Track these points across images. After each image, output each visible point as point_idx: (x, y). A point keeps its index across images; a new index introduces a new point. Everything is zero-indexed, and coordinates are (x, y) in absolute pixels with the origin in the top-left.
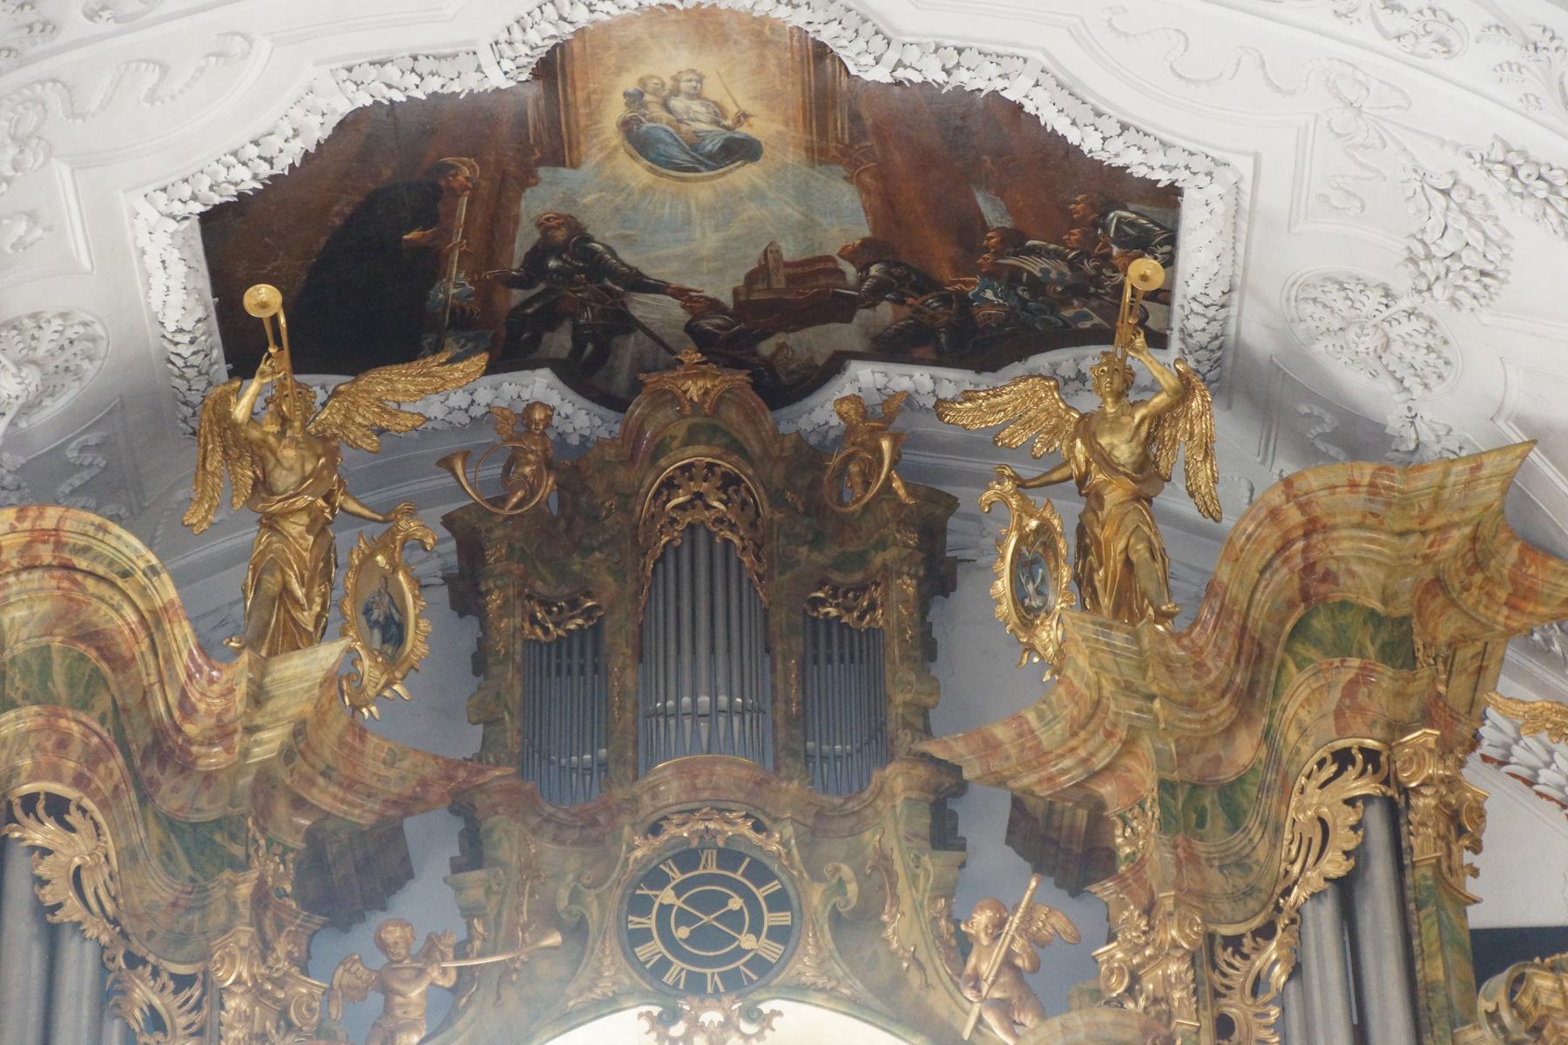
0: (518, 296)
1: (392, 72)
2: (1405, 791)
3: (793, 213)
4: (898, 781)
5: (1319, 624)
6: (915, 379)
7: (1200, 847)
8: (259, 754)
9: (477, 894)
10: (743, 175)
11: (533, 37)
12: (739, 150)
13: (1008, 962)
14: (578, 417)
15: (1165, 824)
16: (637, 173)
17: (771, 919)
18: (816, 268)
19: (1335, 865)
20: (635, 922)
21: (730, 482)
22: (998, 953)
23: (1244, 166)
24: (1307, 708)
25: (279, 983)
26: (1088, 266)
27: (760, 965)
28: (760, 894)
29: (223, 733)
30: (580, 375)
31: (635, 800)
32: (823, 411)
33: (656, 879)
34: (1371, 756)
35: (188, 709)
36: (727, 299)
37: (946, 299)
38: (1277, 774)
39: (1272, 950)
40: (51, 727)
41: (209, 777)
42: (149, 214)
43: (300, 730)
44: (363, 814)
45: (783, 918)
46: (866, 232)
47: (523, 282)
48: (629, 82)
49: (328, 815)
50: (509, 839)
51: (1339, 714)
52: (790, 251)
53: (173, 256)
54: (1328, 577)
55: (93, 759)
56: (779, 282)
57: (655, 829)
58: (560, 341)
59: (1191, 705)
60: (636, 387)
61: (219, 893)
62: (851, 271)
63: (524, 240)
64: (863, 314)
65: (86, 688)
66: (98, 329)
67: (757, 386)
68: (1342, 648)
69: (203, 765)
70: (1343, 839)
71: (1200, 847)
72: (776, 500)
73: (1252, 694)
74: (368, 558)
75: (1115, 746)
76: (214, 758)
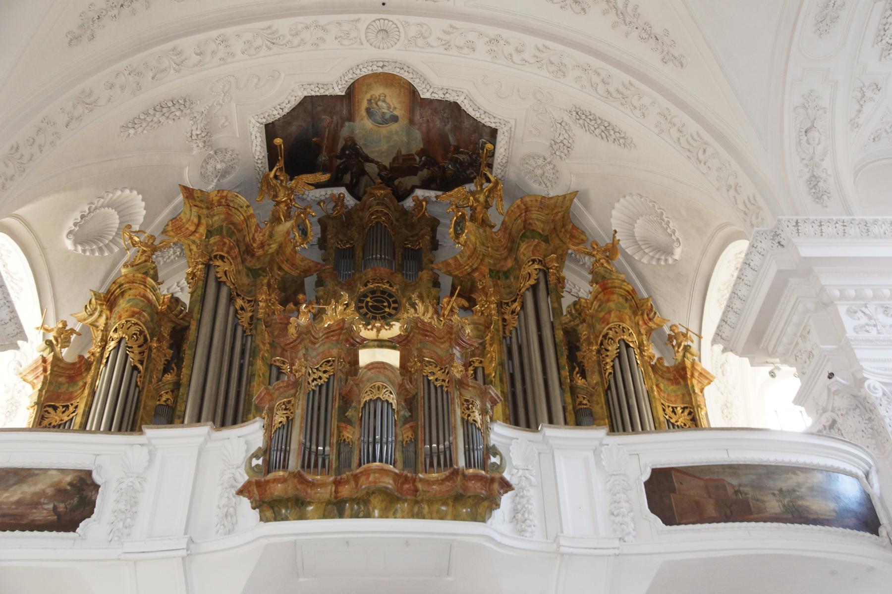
0: (339, 161)
1: (313, 87)
2: (548, 269)
3: (405, 139)
4: (425, 275)
5: (527, 234)
6: (432, 194)
7: (499, 282)
8: (271, 251)
9: (321, 293)
10: (394, 127)
11: (346, 78)
12: (395, 119)
14: (350, 201)
15: (491, 277)
16: (368, 124)
17: (393, 305)
18: (409, 157)
19: (532, 282)
20: (360, 305)
21: (386, 214)
22: (449, 307)
23: (513, 123)
24: (525, 250)
25: (273, 304)
26: (474, 156)
27: (390, 315)
28: (391, 300)
29: (262, 245)
30: (352, 190)
31: (361, 277)
32: (409, 203)
33: (366, 296)
34: (540, 261)
35: (254, 239)
36: (388, 165)
37: (439, 168)
38: (518, 264)
39: (516, 304)
40: (222, 241)
41: (258, 258)
42: (253, 121)
43: (280, 247)
44: (295, 273)
45: (396, 305)
46: (422, 146)
47: (340, 158)
48: (368, 96)
49: (286, 273)
50: (330, 284)
51: (533, 251)
52: (404, 152)
53: (258, 135)
54: (530, 224)
55: (231, 248)
56: (401, 161)
57: (366, 285)
58: (347, 178)
59: (497, 251)
60: (365, 192)
61: (259, 282)
62: (417, 158)
63: (341, 144)
64: (420, 173)
65: (231, 234)
66: (240, 157)
67: (393, 194)
68: (534, 237)
69: (257, 254)
70: (534, 276)
71: (499, 282)
72: (397, 220)
73: (512, 249)
74: (299, 215)
75: (479, 260)
76: (260, 252)
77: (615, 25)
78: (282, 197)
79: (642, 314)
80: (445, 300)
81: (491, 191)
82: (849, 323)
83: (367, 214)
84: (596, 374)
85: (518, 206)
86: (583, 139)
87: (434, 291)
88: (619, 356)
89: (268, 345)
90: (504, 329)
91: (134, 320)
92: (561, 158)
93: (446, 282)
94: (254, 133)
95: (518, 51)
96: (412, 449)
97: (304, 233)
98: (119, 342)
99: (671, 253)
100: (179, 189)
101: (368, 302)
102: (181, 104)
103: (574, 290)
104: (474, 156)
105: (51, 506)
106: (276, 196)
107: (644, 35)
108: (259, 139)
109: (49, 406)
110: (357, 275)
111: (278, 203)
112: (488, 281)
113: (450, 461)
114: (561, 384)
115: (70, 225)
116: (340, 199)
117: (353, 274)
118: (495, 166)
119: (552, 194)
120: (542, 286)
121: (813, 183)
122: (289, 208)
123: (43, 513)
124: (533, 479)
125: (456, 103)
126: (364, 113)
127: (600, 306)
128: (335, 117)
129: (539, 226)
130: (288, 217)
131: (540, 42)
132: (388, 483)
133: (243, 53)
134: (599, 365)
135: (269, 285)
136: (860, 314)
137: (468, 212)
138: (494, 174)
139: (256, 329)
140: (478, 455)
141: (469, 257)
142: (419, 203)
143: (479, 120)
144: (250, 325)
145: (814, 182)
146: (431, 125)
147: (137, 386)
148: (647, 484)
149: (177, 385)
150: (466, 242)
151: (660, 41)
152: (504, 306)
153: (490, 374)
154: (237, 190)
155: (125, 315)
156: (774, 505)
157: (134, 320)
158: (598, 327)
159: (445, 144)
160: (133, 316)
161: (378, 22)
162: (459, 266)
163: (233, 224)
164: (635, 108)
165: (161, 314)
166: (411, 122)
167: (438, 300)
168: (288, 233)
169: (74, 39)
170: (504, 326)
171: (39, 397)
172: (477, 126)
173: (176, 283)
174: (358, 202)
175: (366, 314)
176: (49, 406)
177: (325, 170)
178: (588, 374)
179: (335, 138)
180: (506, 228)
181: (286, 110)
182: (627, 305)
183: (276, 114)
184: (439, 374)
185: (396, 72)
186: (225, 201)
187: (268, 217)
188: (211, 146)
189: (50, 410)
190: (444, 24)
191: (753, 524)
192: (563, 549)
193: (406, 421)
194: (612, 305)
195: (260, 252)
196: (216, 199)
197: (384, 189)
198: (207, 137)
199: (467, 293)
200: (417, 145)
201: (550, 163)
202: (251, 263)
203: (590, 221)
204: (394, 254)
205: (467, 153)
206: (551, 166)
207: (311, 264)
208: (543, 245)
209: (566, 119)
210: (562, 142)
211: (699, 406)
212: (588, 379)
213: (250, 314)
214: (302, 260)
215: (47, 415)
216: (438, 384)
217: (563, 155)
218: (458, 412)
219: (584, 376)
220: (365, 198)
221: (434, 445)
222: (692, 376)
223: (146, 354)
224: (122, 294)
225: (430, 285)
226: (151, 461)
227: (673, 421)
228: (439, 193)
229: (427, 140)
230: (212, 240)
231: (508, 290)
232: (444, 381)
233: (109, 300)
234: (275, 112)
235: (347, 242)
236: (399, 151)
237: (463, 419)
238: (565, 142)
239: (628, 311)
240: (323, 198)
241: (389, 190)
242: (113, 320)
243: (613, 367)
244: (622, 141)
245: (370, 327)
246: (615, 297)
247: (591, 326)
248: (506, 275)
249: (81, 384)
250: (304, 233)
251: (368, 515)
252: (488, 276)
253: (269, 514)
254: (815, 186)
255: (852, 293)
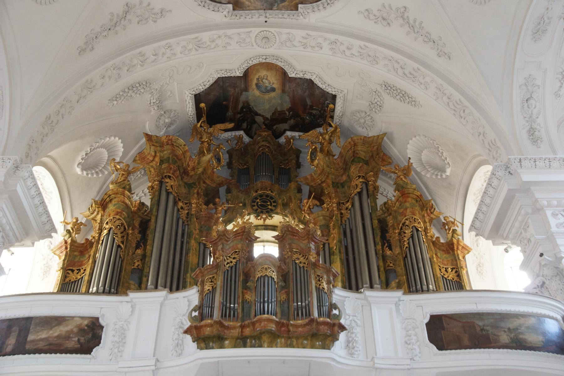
0: (239, 116)
1: (223, 72)
2: (368, 181)
3: (280, 102)
4: (293, 185)
5: (356, 160)
6: (296, 134)
7: (338, 190)
8: (199, 172)
9: (229, 197)
10: (273, 94)
11: (244, 66)
13: (309, 207)
14: (246, 139)
15: (333, 187)
16: (257, 93)
17: (273, 204)
18: (282, 112)
20: (253, 204)
21: (268, 147)
22: (308, 206)
23: (346, 91)
24: (354, 170)
25: (200, 205)
26: (322, 111)
27: (271, 210)
28: (272, 201)
29: (193, 169)
30: (247, 132)
31: (253, 187)
32: (282, 140)
33: (257, 198)
34: (363, 176)
35: (188, 165)
36: (269, 118)
38: (350, 178)
39: (349, 203)
40: (169, 166)
41: (191, 176)
42: (187, 93)
43: (204, 170)
44: (214, 185)
45: (275, 204)
46: (290, 106)
47: (240, 113)
48: (257, 77)
49: (208, 185)
50: (235, 192)
51: (359, 171)
53: (190, 101)
54: (357, 154)
55: (175, 171)
56: (277, 115)
57: (257, 192)
58: (245, 125)
59: (337, 170)
60: (255, 134)
61: (192, 191)
62: (287, 113)
63: (241, 105)
64: (289, 121)
65: (175, 162)
66: (179, 114)
67: (273, 134)
68: (359, 162)
69: (190, 174)
70: (360, 186)
71: (338, 190)
72: (275, 151)
73: (346, 169)
74: (216, 149)
75: (326, 177)
76: (192, 173)
77: (408, 33)
78: (205, 139)
79: (427, 210)
80: (305, 201)
81: (333, 133)
82: (553, 222)
83: (257, 147)
84: (398, 247)
85: (350, 143)
86: (389, 102)
87: (298, 195)
88: (412, 237)
89: (198, 231)
90: (341, 219)
91: (118, 217)
92: (376, 112)
93: (306, 189)
94: (188, 100)
95: (348, 48)
96: (286, 305)
97: (219, 160)
98: (109, 231)
99: (444, 171)
100: (143, 135)
101: (258, 202)
102: (144, 84)
103: (384, 193)
104: (322, 111)
105: (76, 339)
106: (201, 138)
107: (426, 40)
108: (191, 104)
109: (69, 270)
110: (251, 186)
111: (203, 142)
112: (331, 190)
113: (309, 313)
114: (376, 254)
115: (79, 159)
116: (241, 138)
117: (249, 184)
118: (335, 117)
119: (371, 135)
120: (365, 192)
121: (531, 132)
122: (209, 145)
123: (72, 343)
124: (359, 322)
125: (310, 80)
126: (254, 87)
127: (400, 205)
128: (237, 90)
129: (362, 155)
130: (209, 150)
131: (362, 43)
132: (273, 327)
133: (181, 53)
134: (400, 242)
135: (198, 193)
136: (560, 216)
137: (319, 146)
138: (334, 122)
139: (191, 220)
140: (325, 309)
141: (320, 174)
142: (288, 140)
143: (325, 90)
144: (187, 218)
145: (532, 132)
146: (296, 93)
147: (120, 257)
148: (427, 325)
149: (144, 256)
150: (317, 165)
151: (436, 43)
152: (341, 205)
153: (333, 248)
154: (178, 134)
155: (112, 214)
156: (505, 338)
157: (118, 217)
158: (399, 218)
159: (304, 105)
160: (117, 215)
161: (262, 33)
162: (314, 180)
163: (176, 156)
164: (421, 84)
165: (134, 213)
166: (283, 91)
167: (301, 200)
168: (209, 161)
169: (82, 51)
170: (341, 217)
171: (64, 264)
172: (324, 94)
173: (142, 194)
174: (251, 140)
175: (257, 210)
176: (69, 270)
177: (231, 121)
178: (393, 248)
179: (237, 101)
180: (342, 157)
181: (207, 86)
182: (417, 204)
183: (201, 89)
184: (302, 259)
185: (274, 62)
186: (171, 142)
187: (196, 151)
188: (162, 108)
189: (70, 272)
190: (303, 33)
191: (492, 350)
192: (376, 365)
193: (282, 288)
194: (408, 204)
195: (192, 173)
196: (165, 141)
197: (267, 132)
198: (160, 103)
199: (318, 196)
200: (287, 105)
201: (369, 116)
202: (186, 179)
203: (394, 151)
204: (274, 171)
205: (318, 110)
206: (370, 118)
207: (223, 180)
208: (365, 166)
209: (379, 89)
210: (376, 103)
211: (462, 267)
212: (393, 251)
213: (187, 212)
214: (218, 178)
215: (68, 275)
216: (301, 265)
217: (377, 111)
218: (314, 282)
219: (390, 249)
220: (255, 137)
221: (299, 303)
222: (458, 248)
223: (125, 238)
224: (111, 201)
225: (296, 191)
226: (133, 312)
227: (446, 276)
228: (301, 134)
229: (293, 101)
230: (164, 166)
231: (344, 195)
232: (305, 263)
233: (103, 205)
234: (201, 87)
235: (245, 164)
236: (276, 109)
237: (316, 287)
238: (378, 103)
239: (418, 208)
240: (230, 138)
241: (270, 132)
242: (105, 217)
243: (409, 243)
244: (413, 103)
245: (259, 218)
246: (410, 199)
247: (395, 218)
248: (343, 185)
249: (87, 256)
250: (219, 160)
251: (260, 346)
252: (331, 186)
253: (203, 345)
254: (532, 134)
255: (555, 203)
